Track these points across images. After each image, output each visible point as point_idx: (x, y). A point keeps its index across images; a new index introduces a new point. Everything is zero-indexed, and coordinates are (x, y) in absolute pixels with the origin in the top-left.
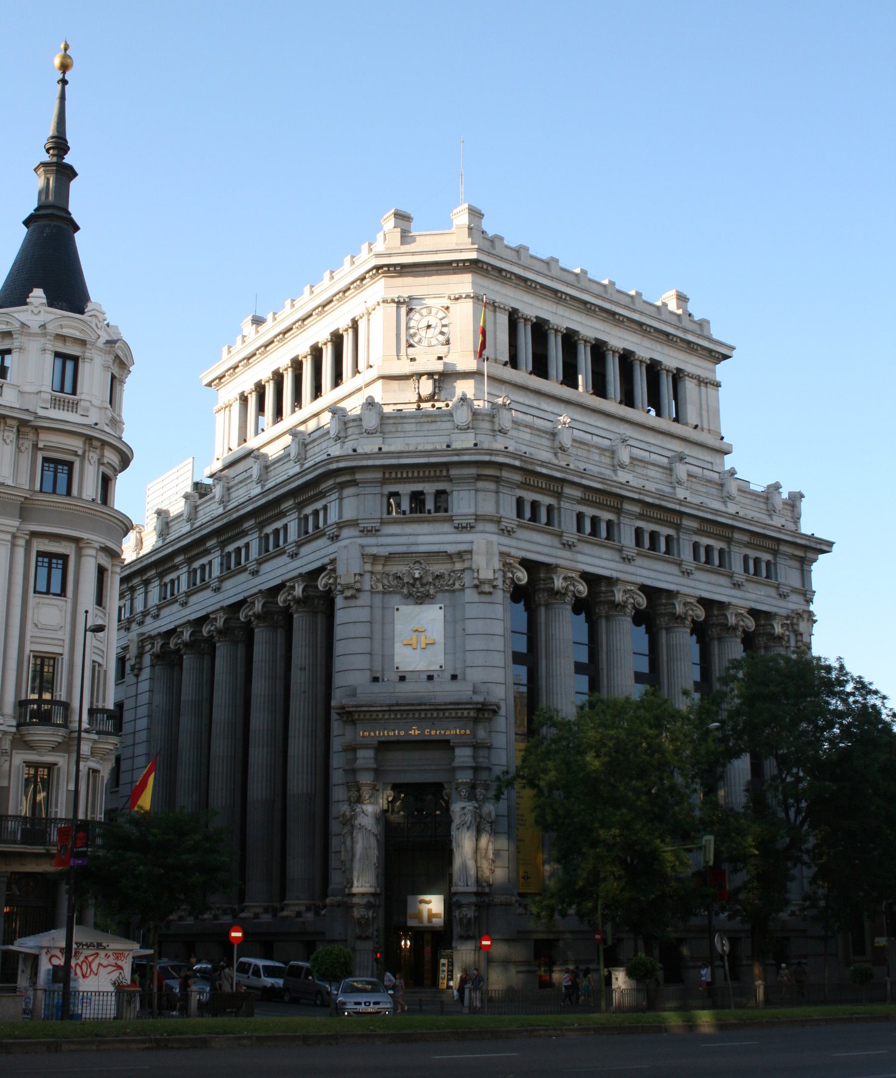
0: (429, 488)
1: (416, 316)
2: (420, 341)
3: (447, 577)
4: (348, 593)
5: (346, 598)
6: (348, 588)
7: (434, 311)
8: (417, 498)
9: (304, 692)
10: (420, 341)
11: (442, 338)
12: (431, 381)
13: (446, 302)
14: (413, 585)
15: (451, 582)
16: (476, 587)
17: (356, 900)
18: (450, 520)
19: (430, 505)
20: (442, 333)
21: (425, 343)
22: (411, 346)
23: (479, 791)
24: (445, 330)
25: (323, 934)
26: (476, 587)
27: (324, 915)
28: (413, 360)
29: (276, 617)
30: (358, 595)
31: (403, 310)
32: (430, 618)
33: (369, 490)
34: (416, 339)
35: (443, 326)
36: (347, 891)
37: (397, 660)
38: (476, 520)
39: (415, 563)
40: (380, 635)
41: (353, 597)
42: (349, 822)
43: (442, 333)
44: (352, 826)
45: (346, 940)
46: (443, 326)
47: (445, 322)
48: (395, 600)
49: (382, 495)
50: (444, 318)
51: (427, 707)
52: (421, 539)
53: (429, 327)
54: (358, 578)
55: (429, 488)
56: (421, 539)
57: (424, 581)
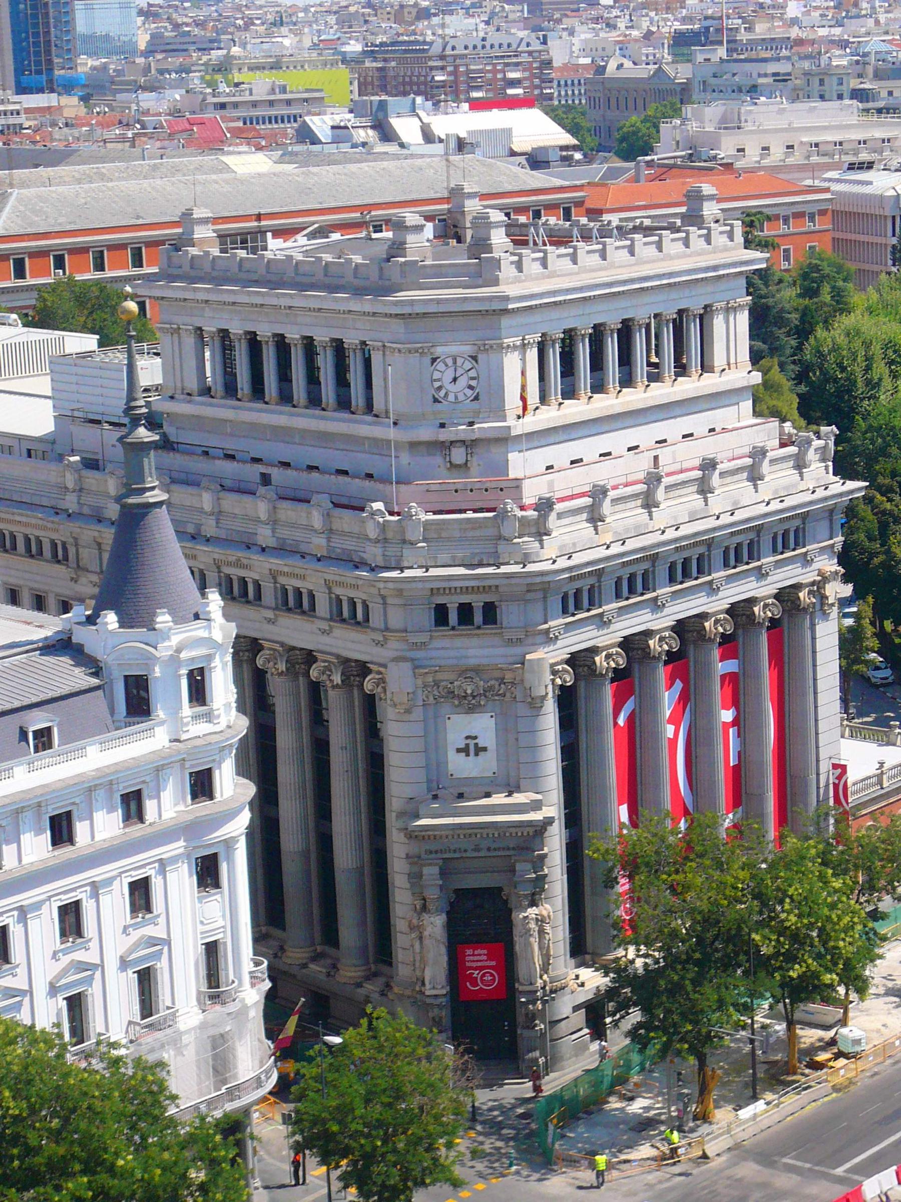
2: (446, 395)
7: (460, 361)
10: (446, 395)
11: (469, 392)
12: (463, 450)
17: (428, 1001)
19: (478, 618)
20: (471, 387)
21: (451, 398)
22: (436, 400)
24: (473, 383)
28: (442, 426)
31: (427, 360)
32: (484, 726)
34: (442, 393)
35: (473, 378)
37: (451, 768)
40: (432, 746)
42: (417, 929)
43: (471, 387)
46: (473, 378)
47: (472, 373)
48: (445, 708)
52: (471, 652)
53: (455, 380)
56: (471, 652)
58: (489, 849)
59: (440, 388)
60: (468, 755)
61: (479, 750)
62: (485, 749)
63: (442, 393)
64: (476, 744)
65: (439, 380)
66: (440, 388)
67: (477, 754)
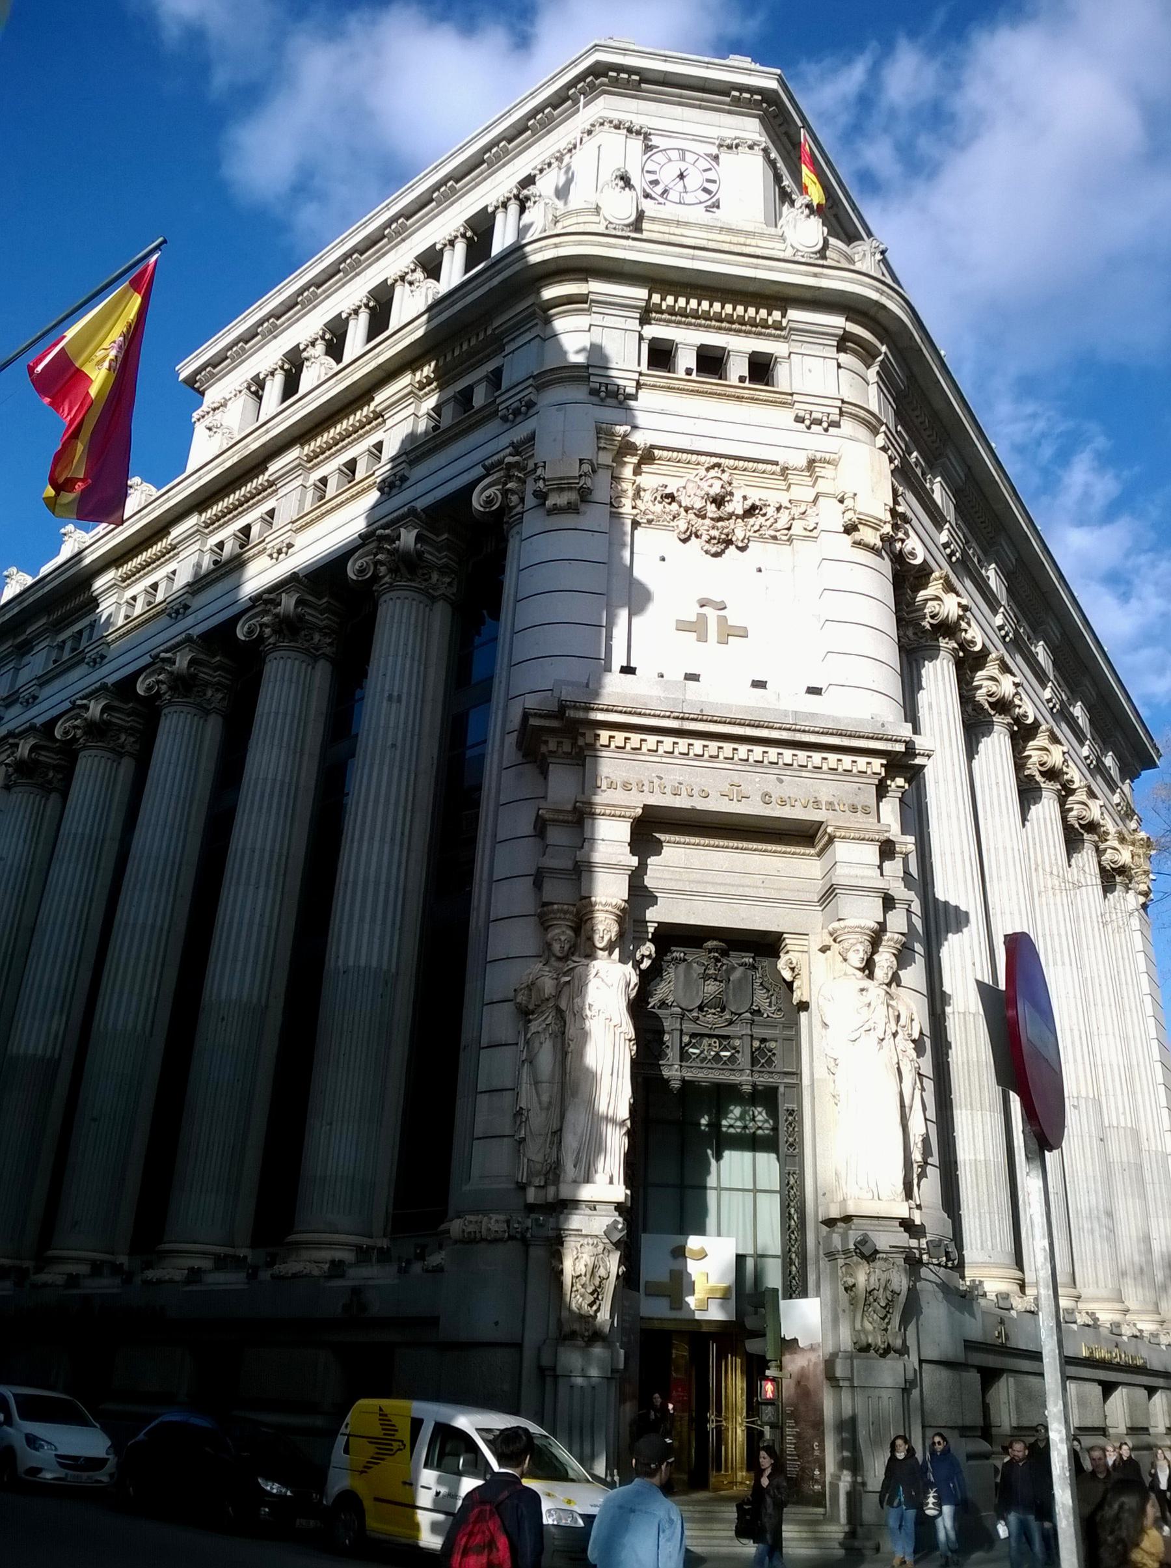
0: (740, 346)
1: (659, 158)
3: (770, 511)
4: (560, 499)
5: (556, 510)
6: (561, 490)
7: (690, 157)
8: (711, 362)
9: (394, 746)
13: (714, 150)
14: (701, 515)
15: (779, 525)
16: (850, 529)
18: (786, 400)
20: (706, 190)
23: (885, 959)
24: (709, 186)
25: (432, 1322)
26: (850, 529)
27: (439, 1269)
29: (317, 637)
30: (583, 507)
33: (609, 321)
34: (659, 189)
35: (708, 181)
36: (531, 1195)
38: (841, 413)
39: (708, 470)
41: (571, 509)
43: (706, 190)
44: (560, 1012)
45: (518, 1346)
46: (708, 181)
47: (711, 175)
49: (641, 338)
50: (710, 169)
51: (775, 734)
54: (586, 468)
55: (740, 346)
57: (729, 508)
58: (766, 798)
59: (655, 183)
60: (702, 638)
61: (729, 632)
62: (743, 633)
63: (659, 189)
64: (723, 620)
65: (654, 172)
66: (655, 183)
67: (723, 642)
